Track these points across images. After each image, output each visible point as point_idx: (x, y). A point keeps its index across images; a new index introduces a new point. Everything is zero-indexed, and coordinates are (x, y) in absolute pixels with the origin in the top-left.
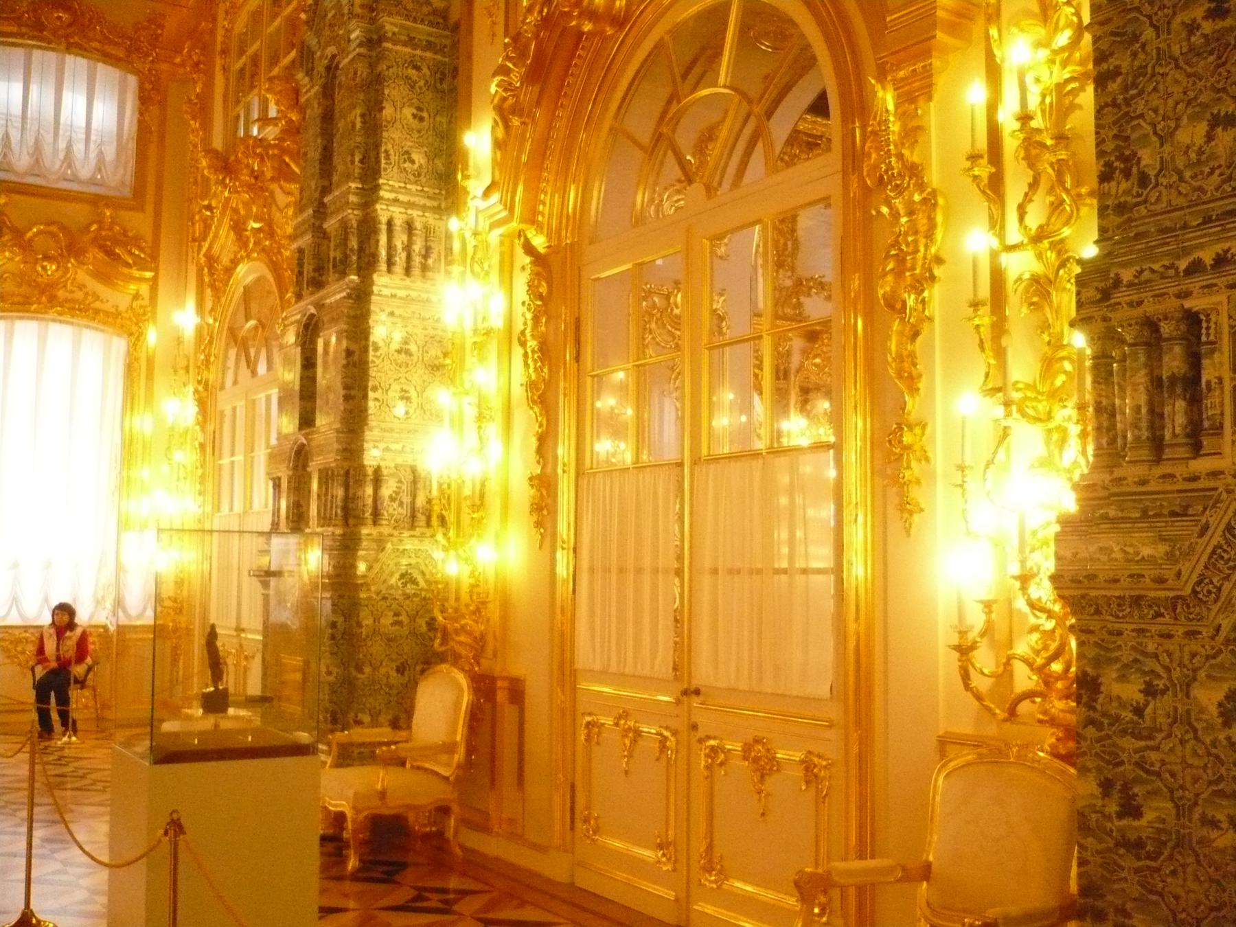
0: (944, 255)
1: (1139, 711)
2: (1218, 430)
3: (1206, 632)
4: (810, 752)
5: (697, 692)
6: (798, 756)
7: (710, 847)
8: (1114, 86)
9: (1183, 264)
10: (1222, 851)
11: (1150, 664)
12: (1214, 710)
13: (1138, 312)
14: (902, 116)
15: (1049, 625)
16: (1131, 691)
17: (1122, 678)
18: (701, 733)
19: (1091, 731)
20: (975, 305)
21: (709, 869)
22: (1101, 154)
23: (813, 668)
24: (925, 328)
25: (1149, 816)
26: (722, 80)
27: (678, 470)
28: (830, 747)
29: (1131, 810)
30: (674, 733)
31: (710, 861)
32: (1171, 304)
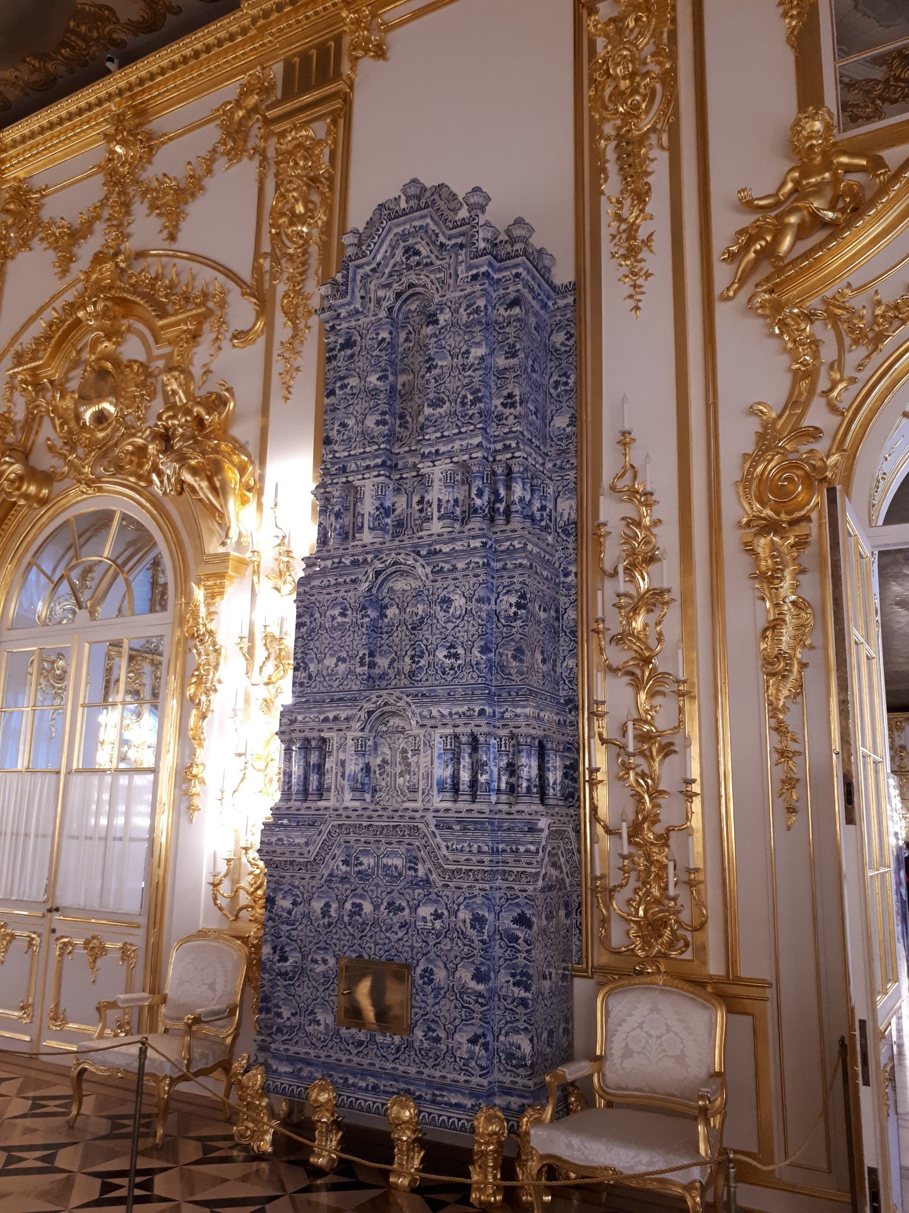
0: (222, 679)
1: (289, 913)
2: (329, 790)
3: (318, 877)
4: (126, 943)
5: (57, 910)
6: (120, 945)
7: (57, 1005)
8: (303, 630)
9: (322, 717)
10: (318, 974)
11: (296, 891)
12: (319, 911)
13: (303, 735)
14: (208, 605)
15: (258, 871)
16: (287, 904)
17: (284, 898)
18: (57, 935)
19: (270, 923)
20: (241, 638)
21: (55, 1019)
22: (295, 659)
23: (129, 895)
24: (209, 715)
25: (291, 960)
26: (106, 554)
27: (55, 776)
28: (138, 939)
29: (284, 959)
30: (39, 936)
31: (56, 1014)
32: (315, 734)
